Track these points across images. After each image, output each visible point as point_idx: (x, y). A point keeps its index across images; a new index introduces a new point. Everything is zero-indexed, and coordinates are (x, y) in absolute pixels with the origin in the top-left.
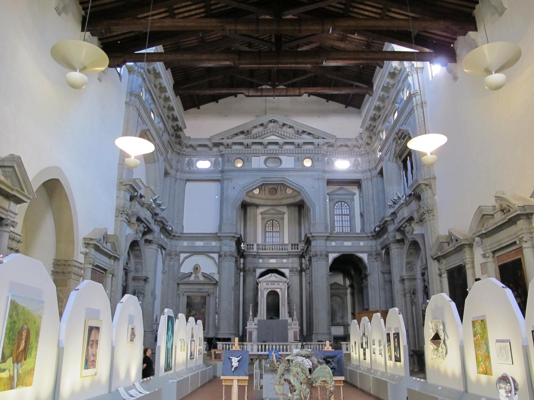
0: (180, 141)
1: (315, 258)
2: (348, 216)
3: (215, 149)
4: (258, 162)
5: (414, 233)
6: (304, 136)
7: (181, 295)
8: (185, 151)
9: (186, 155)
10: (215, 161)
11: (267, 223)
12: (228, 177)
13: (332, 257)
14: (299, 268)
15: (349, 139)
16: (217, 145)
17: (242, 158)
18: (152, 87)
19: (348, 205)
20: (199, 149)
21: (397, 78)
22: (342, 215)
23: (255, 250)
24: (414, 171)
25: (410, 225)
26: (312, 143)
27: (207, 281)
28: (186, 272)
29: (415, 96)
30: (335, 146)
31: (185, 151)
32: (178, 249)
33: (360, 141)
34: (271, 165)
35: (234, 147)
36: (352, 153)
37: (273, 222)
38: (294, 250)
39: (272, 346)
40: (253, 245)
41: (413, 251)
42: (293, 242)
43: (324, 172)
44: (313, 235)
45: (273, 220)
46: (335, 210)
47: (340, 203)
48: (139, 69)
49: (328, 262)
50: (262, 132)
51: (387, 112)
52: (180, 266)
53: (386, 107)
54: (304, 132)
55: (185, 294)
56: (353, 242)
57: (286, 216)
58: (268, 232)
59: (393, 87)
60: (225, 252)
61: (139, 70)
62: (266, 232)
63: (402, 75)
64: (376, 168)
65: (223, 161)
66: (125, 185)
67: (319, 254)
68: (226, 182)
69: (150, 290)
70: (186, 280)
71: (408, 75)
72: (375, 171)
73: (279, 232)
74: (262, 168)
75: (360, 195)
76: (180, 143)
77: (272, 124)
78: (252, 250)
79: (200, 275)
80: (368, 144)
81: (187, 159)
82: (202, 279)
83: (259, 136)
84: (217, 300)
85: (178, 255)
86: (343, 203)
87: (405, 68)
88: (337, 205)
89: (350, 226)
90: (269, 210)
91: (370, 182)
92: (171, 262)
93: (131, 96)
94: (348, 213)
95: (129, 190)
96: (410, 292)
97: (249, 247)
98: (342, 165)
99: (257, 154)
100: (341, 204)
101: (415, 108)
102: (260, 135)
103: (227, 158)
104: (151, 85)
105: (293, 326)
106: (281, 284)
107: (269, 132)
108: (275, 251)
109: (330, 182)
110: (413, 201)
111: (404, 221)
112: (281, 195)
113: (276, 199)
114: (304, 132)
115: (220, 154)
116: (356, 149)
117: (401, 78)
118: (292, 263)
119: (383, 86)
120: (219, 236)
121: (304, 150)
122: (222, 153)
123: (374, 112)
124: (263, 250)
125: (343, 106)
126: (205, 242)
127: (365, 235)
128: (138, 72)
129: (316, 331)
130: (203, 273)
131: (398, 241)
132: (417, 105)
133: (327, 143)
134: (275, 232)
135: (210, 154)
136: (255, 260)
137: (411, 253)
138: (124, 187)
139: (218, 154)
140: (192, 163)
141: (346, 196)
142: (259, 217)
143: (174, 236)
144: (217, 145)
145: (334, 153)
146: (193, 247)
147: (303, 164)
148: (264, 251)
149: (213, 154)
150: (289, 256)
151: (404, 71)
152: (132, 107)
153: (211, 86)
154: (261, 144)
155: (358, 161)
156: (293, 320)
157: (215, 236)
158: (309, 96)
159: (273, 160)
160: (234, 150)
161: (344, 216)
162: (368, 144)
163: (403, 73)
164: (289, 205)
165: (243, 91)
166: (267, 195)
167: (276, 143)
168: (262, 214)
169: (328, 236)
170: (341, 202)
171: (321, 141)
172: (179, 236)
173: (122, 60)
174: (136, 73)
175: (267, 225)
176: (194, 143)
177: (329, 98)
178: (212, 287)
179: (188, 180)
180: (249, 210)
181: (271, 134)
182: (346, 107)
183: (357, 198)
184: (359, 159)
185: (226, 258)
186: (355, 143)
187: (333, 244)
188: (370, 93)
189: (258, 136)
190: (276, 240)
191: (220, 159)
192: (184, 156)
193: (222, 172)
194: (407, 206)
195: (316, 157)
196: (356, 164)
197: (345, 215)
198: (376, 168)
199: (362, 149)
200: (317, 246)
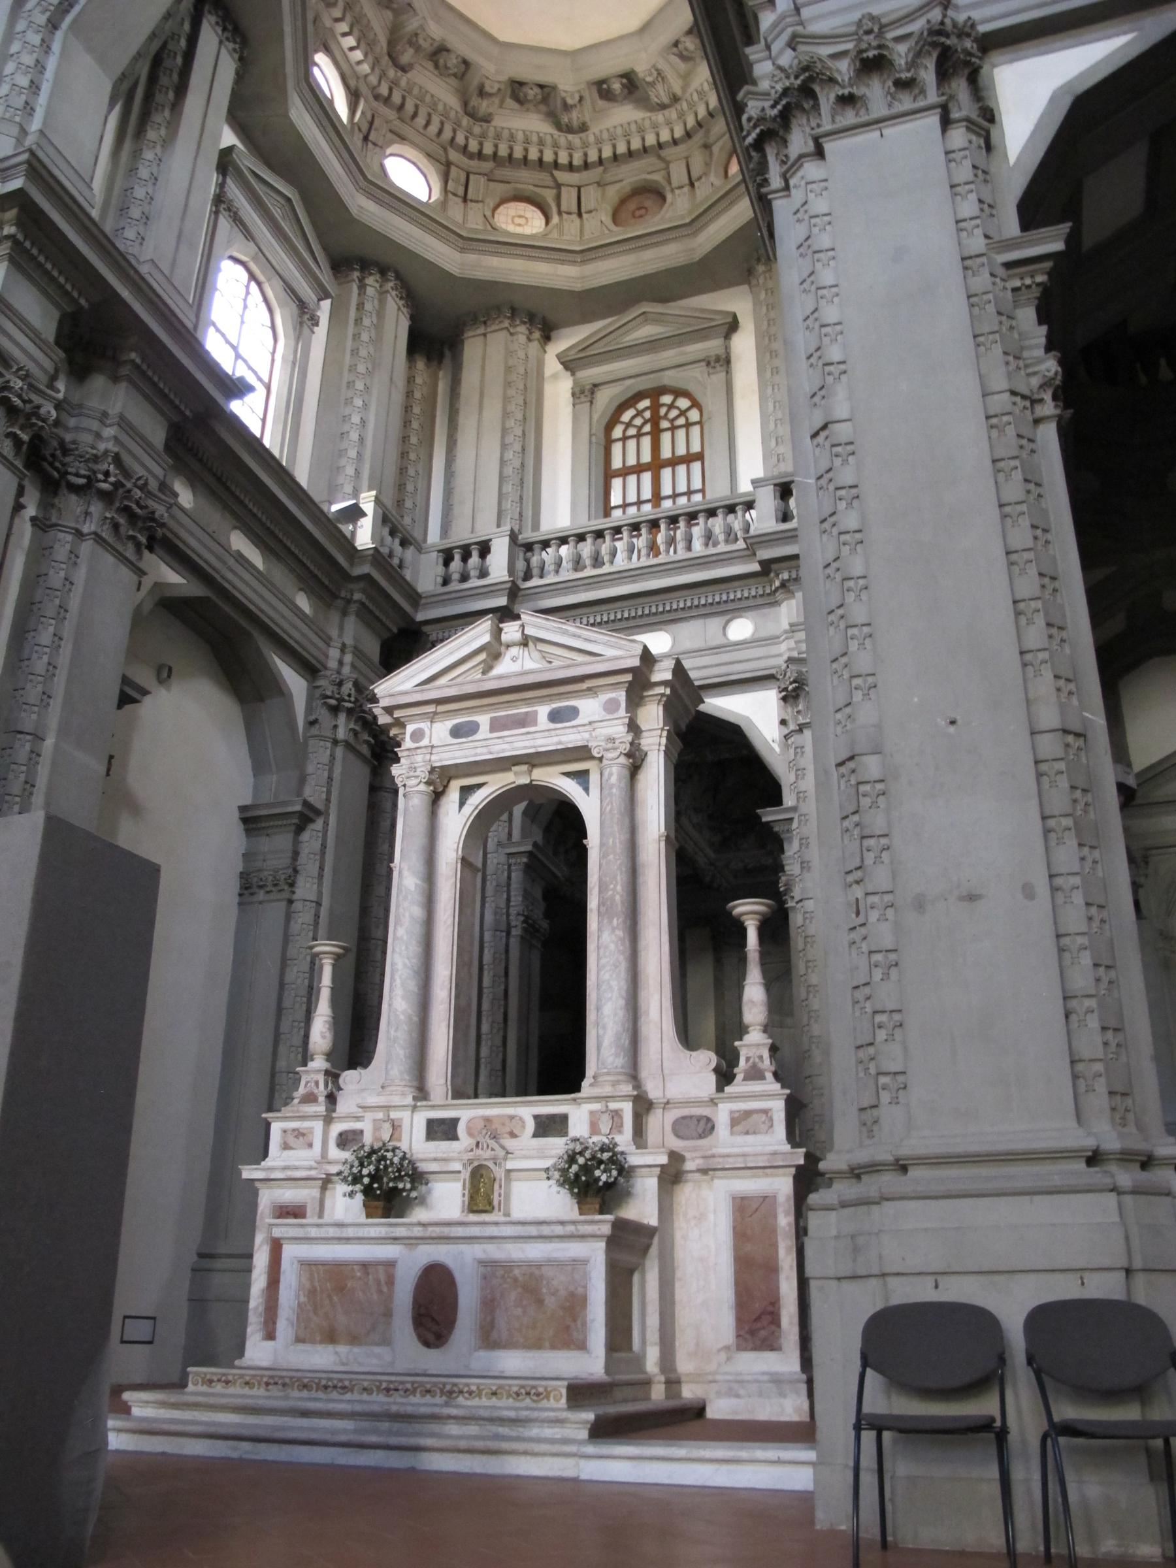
37: (655, 407)
40: (485, 549)
62: (609, 475)
97: (456, 565)
105: (725, 1141)
106: (589, 707)
129: (869, 1124)
134: (674, 462)
142: (559, 391)
156: (725, 1076)
175: (617, 432)
180: (488, 354)
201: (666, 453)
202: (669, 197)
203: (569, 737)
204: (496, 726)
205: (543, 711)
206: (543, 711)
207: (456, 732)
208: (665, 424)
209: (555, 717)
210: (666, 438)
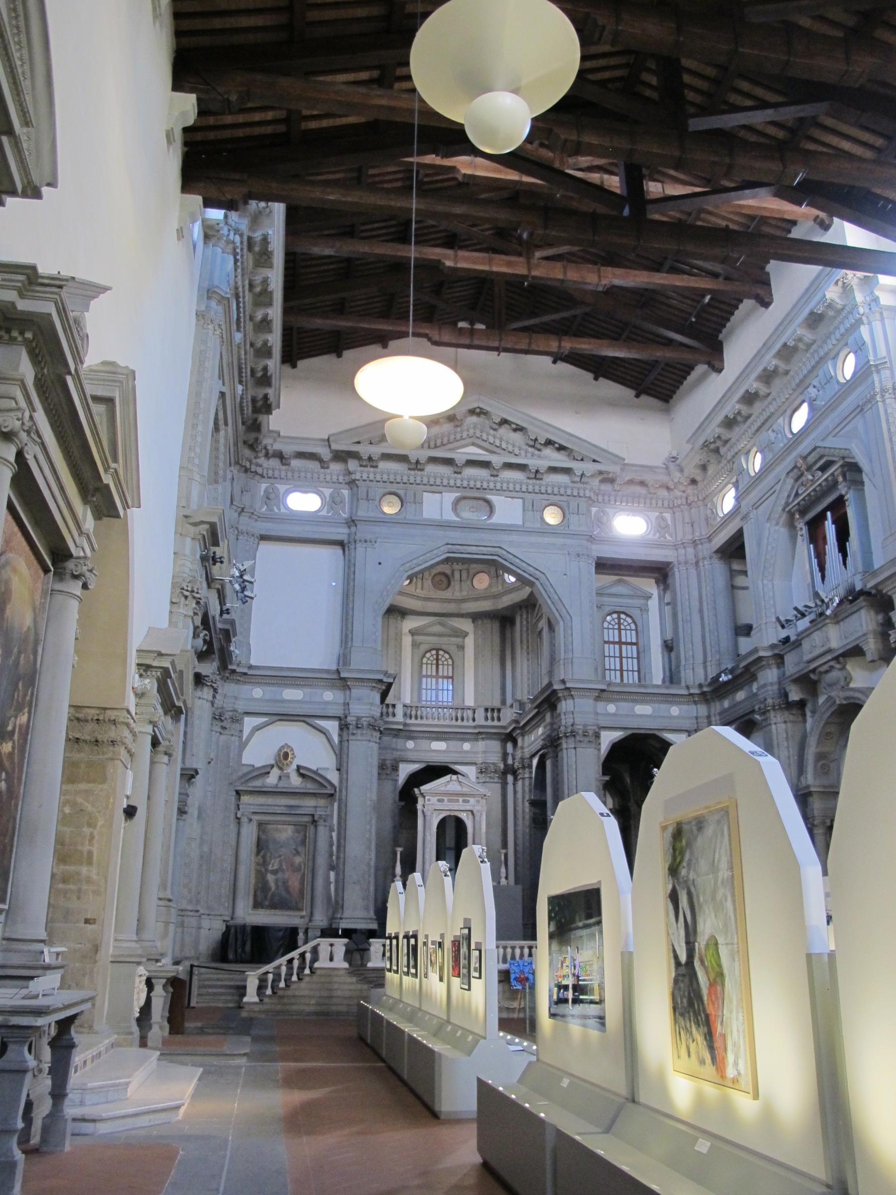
0: (257, 439)
1: (571, 740)
2: (634, 647)
3: (336, 467)
4: (437, 506)
5: (852, 685)
6: (548, 452)
7: (244, 820)
8: (261, 466)
9: (262, 476)
10: (332, 496)
11: (424, 656)
12: (368, 537)
13: (608, 738)
14: (502, 766)
15: (651, 469)
16: (341, 456)
17: (401, 492)
18: (243, 287)
19: (634, 622)
20: (295, 463)
21: (822, 329)
22: (620, 643)
23: (399, 717)
24: (853, 544)
25: (843, 668)
26: (567, 471)
27: (310, 787)
28: (257, 765)
29: (878, 372)
30: (618, 481)
31: (261, 466)
32: (241, 707)
33: (677, 475)
34: (469, 514)
35: (383, 465)
36: (654, 502)
37: (437, 655)
38: (489, 723)
39: (513, 948)
40: (394, 706)
41: (832, 729)
42: (489, 704)
43: (591, 539)
44: (568, 685)
45: (437, 650)
46: (606, 631)
47: (615, 616)
48: (232, 233)
49: (599, 750)
50: (449, 434)
51: (772, 409)
52: (243, 745)
53: (774, 394)
54: (549, 443)
55: (255, 818)
56: (656, 705)
57: (469, 642)
58: (427, 676)
59: (807, 351)
60: (359, 718)
61: (231, 237)
62: (421, 677)
63: (842, 322)
65: (355, 498)
66: (195, 524)
67: (579, 728)
68: (360, 548)
69: (196, 805)
70: (258, 783)
71: (859, 322)
72: (707, 545)
73: (452, 678)
74: (448, 521)
75: (661, 599)
76: (252, 446)
77: (474, 419)
78: (391, 719)
79: (291, 770)
80: (694, 482)
81: (264, 486)
82: (296, 781)
83: (443, 445)
84: (334, 835)
85: (237, 720)
86: (623, 616)
87: (855, 306)
88: (609, 618)
89: (639, 671)
90: (430, 625)
91: (693, 572)
92: (223, 738)
93: (209, 298)
94: (634, 641)
95: (204, 537)
96: (824, 823)
98: (630, 527)
99: (436, 487)
100: (619, 618)
101: (878, 398)
102: (445, 441)
103: (365, 490)
104: (243, 281)
106: (472, 800)
107: (465, 435)
108: (444, 721)
109: (603, 566)
110: (863, 612)
111: (829, 657)
112: (461, 591)
113: (449, 601)
114: (549, 443)
115: (348, 479)
116: (664, 493)
117: (837, 328)
118: (484, 752)
119: (785, 345)
120: (344, 679)
121: (547, 486)
122: (353, 477)
123: (738, 406)
124: (416, 718)
125: (630, 393)
126: (308, 690)
127: (685, 692)
128: (228, 242)
130: (299, 768)
131: (789, 705)
132: (883, 391)
133: (601, 473)
135: (322, 476)
136: (399, 743)
137: (828, 734)
138: (192, 529)
139: (341, 478)
140: (278, 496)
141: (630, 601)
142: (407, 640)
143: (234, 671)
144: (341, 456)
145: (612, 498)
146: (276, 701)
147: (542, 519)
148: (419, 721)
149: (328, 478)
150: (478, 735)
151: (851, 312)
152: (211, 327)
153: (340, 309)
154: (449, 462)
155: (664, 519)
157: (335, 676)
158: (554, 362)
159: (475, 503)
160: (382, 473)
161: (624, 647)
162: (694, 482)
163: (846, 317)
164: (476, 617)
165: (427, 331)
166: (426, 589)
167: (486, 465)
168: (413, 633)
169: (603, 691)
170: (619, 613)
171: (589, 468)
172: (245, 674)
173: (245, 190)
174: (222, 243)
175: (425, 660)
176: (289, 449)
177: (600, 368)
178: (322, 802)
179: (263, 538)
181: (470, 440)
182: (637, 396)
183: (653, 604)
184: (668, 516)
185: (359, 731)
186: (664, 478)
187: (611, 708)
188: (717, 364)
189: (439, 443)
190: (446, 697)
191: (346, 492)
192: (257, 477)
193: (352, 522)
194: (838, 622)
195: (573, 504)
196: (661, 526)
197: (626, 643)
198: (710, 539)
199: (678, 493)
200: (575, 711)
201: (440, 674)
202: (452, 583)
203: (468, 807)
204: (449, 801)
205: (461, 799)
206: (461, 799)
207: (439, 800)
208: (440, 662)
209: (464, 801)
210: (441, 667)
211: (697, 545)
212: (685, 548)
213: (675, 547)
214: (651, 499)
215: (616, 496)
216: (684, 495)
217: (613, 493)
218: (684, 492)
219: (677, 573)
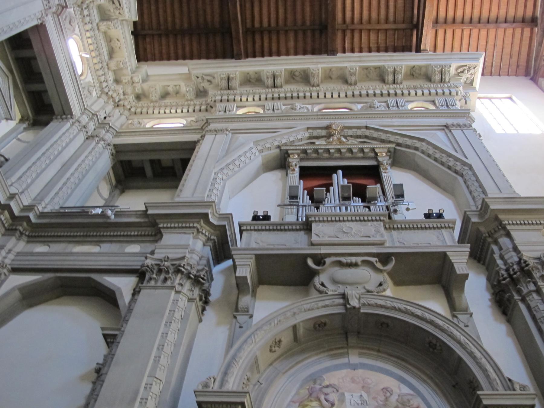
36: (101, 72)
64: (118, 134)
80: (138, 97)
91: (81, 137)
116: (111, 77)
211: (104, 128)
212: (91, 119)
213: (85, 110)
214: (102, 68)
215: (92, 29)
216: (122, 97)
217: (95, 25)
218: (124, 94)
219: (68, 125)
